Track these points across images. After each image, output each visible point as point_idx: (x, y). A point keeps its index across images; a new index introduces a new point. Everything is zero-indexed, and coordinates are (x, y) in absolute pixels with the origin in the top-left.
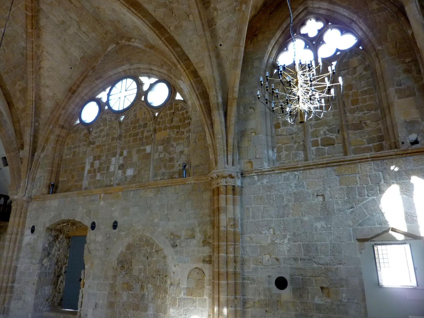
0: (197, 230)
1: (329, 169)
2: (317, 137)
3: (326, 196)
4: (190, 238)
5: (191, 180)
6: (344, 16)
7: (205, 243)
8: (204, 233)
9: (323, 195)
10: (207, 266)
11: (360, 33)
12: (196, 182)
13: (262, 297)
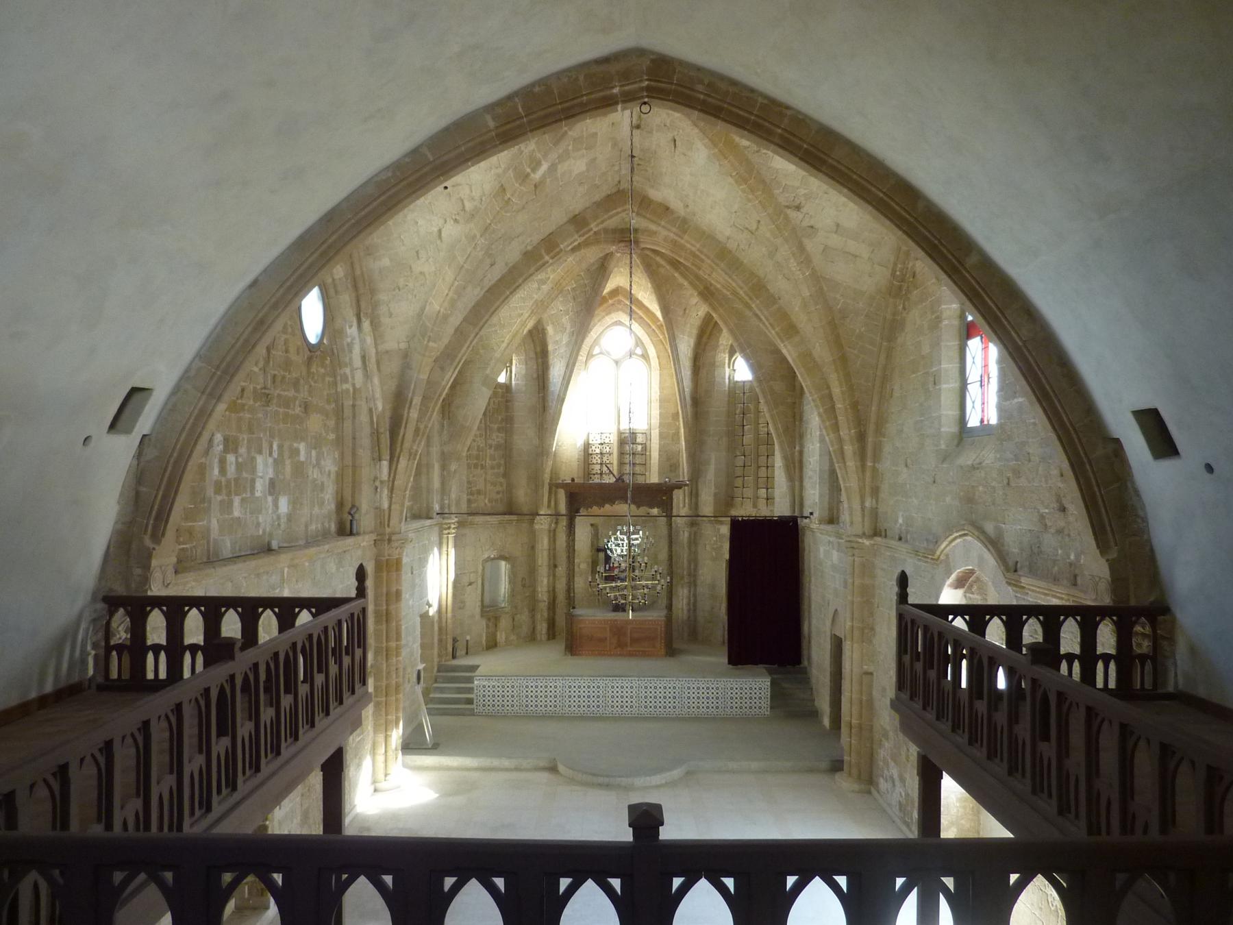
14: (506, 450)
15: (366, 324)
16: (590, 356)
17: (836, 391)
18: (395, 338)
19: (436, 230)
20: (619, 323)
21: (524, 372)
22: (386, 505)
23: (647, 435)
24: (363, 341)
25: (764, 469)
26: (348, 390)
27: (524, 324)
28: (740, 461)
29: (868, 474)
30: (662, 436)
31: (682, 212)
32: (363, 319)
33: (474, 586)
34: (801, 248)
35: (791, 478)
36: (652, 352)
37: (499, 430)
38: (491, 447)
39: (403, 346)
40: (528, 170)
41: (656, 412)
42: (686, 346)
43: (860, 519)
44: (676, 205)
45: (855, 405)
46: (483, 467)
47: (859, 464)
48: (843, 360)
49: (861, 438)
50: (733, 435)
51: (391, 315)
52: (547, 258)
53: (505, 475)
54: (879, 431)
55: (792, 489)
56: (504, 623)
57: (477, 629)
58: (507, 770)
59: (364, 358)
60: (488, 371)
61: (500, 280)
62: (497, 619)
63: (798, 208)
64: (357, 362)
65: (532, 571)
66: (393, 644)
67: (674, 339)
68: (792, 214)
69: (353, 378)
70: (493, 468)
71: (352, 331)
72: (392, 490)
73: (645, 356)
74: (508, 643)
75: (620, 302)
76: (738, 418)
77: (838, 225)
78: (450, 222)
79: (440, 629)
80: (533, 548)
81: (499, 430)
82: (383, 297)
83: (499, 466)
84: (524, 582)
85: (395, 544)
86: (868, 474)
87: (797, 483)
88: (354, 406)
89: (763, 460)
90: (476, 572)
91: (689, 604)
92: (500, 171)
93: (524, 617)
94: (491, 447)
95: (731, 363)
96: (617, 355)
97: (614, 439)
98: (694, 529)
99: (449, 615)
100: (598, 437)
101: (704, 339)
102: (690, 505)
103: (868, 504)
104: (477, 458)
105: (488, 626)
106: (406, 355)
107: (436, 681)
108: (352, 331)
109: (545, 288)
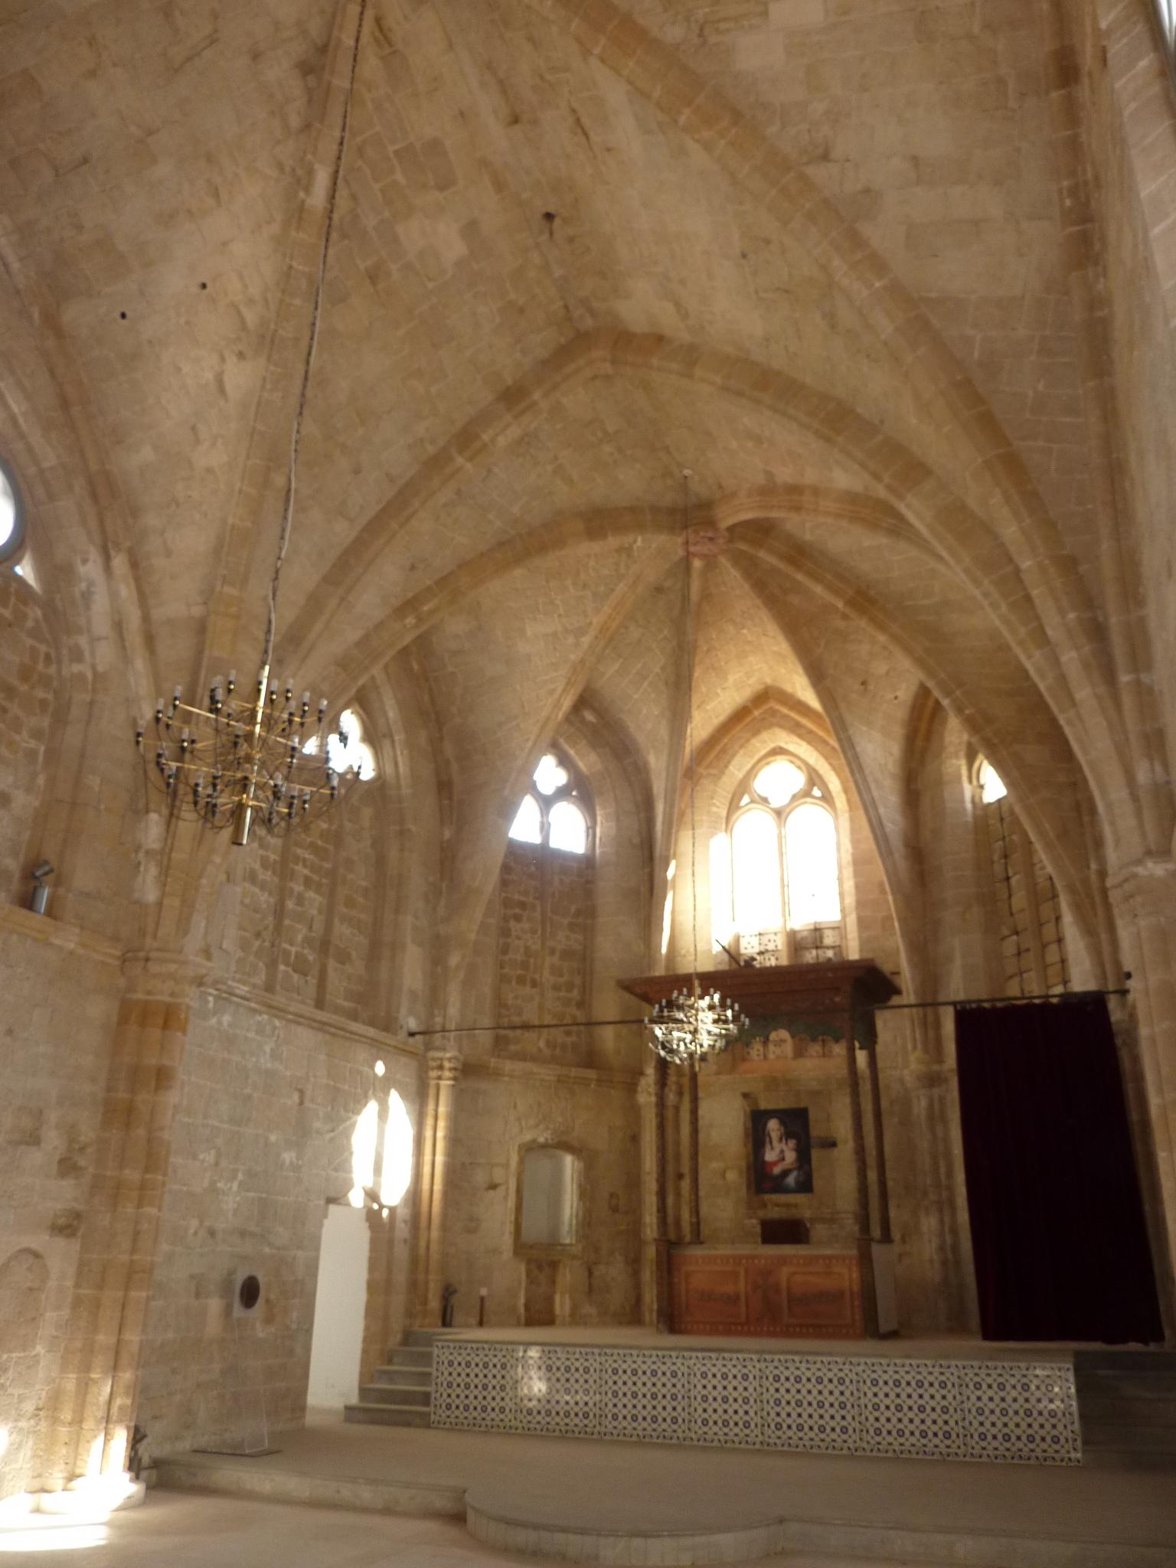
0: (53, 1116)
1: (320, 1035)
2: (291, 945)
3: (308, 1093)
4: (28, 1144)
5: (68, 939)
6: (385, 713)
7: (67, 1167)
8: (71, 1133)
9: (301, 1092)
10: (61, 1242)
11: (389, 770)
12: (81, 951)
13: (170, 1335)
14: (583, 961)
15: (119, 562)
16: (733, 806)
17: (1010, 532)
18: (179, 599)
19: (209, 376)
20: (778, 751)
21: (613, 832)
22: (151, 896)
23: (839, 929)
24: (113, 595)
25: (1054, 947)
26: (81, 676)
27: (557, 705)
28: (1010, 946)
29: (1128, 701)
30: (862, 923)
31: (686, 337)
32: (112, 553)
33: (501, 1191)
34: (856, 241)
35: (1089, 930)
36: (834, 784)
37: (572, 927)
38: (553, 952)
39: (197, 611)
40: (302, 195)
41: (849, 884)
42: (881, 750)
43: (1132, 822)
44: (668, 320)
45: (1069, 565)
46: (534, 984)
47: (1102, 690)
48: (1011, 467)
49: (1097, 632)
50: (991, 900)
51: (169, 554)
52: (460, 460)
53: (581, 1004)
54: (1132, 591)
55: (1096, 950)
56: (569, 1276)
57: (507, 1277)
58: (365, 1510)
59: (118, 626)
60: (506, 792)
61: (383, 510)
62: (554, 1265)
63: (825, 157)
64: (101, 624)
65: (633, 1182)
66: (132, 1175)
67: (845, 729)
68: (818, 173)
69: (93, 654)
70: (556, 988)
71: (90, 569)
72: (165, 871)
73: (827, 798)
74: (577, 1319)
75: (774, 713)
76: (998, 868)
77: (915, 160)
78: (231, 360)
79: (414, 1260)
80: (635, 1139)
81: (572, 927)
82: (152, 520)
83: (570, 986)
84: (610, 1204)
85: (154, 968)
86: (1128, 701)
87: (1104, 937)
88: (91, 703)
89: (1049, 931)
90: (507, 1166)
91: (941, 1248)
92: (275, 228)
93: (615, 1271)
94: (553, 952)
95: (973, 776)
96: (777, 802)
97: (779, 943)
98: (936, 1092)
99: (435, 1234)
100: (755, 941)
101: (919, 743)
102: (925, 1043)
103: (1142, 776)
104: (524, 965)
105: (531, 1280)
106: (201, 628)
107: (390, 1362)
108: (90, 569)
109: (586, 640)
